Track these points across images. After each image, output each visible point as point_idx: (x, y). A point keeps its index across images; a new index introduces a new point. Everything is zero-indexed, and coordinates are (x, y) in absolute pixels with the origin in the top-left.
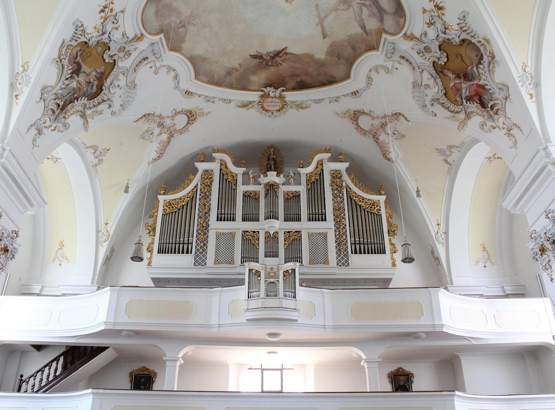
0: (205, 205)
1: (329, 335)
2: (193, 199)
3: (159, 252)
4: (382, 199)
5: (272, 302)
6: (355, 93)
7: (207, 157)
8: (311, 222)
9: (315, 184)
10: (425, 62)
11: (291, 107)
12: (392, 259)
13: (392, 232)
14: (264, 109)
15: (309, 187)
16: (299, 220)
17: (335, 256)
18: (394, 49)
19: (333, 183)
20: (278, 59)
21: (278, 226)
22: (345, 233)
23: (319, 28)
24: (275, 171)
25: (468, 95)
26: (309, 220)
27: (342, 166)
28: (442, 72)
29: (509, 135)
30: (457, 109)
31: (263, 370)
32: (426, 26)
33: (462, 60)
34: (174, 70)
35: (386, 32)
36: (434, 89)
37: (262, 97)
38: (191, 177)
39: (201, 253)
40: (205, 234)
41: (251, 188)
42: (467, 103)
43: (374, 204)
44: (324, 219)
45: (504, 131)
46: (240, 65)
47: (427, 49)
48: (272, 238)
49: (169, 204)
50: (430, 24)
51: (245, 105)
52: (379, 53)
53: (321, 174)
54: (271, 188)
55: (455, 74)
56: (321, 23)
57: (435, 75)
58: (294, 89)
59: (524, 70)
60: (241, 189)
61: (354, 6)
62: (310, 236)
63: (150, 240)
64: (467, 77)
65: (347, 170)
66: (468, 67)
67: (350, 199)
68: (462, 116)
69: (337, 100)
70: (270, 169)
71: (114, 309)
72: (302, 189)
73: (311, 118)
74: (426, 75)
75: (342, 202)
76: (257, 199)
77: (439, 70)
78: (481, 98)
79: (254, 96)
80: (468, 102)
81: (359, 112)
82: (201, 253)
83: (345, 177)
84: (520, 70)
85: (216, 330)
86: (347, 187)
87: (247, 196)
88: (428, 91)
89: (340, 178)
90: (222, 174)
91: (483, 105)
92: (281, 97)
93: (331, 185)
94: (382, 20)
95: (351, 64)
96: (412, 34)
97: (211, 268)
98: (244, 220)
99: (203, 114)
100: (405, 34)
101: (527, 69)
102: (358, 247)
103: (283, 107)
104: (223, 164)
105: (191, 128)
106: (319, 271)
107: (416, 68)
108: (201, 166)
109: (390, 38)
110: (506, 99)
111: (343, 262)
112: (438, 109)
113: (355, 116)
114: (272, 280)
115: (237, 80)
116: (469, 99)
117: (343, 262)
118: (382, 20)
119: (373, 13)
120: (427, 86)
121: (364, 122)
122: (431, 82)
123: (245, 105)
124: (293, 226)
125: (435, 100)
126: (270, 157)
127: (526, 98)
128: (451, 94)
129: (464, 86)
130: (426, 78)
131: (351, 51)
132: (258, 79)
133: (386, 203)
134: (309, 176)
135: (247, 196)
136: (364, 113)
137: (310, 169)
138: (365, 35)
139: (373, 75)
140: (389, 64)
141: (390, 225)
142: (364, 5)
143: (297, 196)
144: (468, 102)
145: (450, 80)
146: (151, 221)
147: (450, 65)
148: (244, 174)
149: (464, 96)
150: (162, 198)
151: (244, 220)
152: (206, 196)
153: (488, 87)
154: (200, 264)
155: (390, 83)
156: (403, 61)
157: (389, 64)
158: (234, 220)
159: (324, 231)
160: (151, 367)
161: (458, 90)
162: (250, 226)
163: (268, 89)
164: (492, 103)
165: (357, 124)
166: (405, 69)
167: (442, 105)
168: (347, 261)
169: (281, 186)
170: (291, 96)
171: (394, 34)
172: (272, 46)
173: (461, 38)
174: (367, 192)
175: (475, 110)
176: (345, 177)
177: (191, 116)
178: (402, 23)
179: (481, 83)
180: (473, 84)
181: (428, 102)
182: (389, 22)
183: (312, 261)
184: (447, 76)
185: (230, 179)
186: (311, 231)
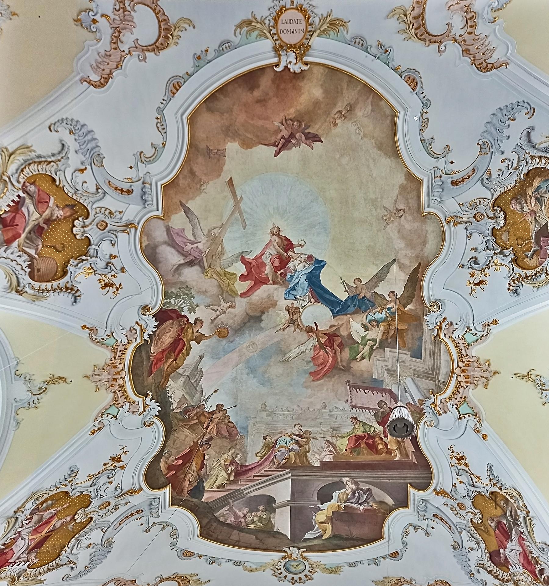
25: (23, 209)
33: (55, 248)
35: (158, 218)
42: (19, 196)
55: (55, 220)
56: (237, 202)
61: (203, 237)
66: (43, 247)
80: (16, 199)
94: (168, 230)
95: (192, 145)
119: (181, 236)
128: (46, 186)
129: (36, 215)
131: (196, 169)
138: (184, 202)
142: (192, 243)
144: (16, 199)
145: (57, 206)
147: (65, 227)
149: (28, 201)
156: (126, 187)
161: (41, 202)
178: (145, 239)
180: (24, 232)
184: (63, 209)
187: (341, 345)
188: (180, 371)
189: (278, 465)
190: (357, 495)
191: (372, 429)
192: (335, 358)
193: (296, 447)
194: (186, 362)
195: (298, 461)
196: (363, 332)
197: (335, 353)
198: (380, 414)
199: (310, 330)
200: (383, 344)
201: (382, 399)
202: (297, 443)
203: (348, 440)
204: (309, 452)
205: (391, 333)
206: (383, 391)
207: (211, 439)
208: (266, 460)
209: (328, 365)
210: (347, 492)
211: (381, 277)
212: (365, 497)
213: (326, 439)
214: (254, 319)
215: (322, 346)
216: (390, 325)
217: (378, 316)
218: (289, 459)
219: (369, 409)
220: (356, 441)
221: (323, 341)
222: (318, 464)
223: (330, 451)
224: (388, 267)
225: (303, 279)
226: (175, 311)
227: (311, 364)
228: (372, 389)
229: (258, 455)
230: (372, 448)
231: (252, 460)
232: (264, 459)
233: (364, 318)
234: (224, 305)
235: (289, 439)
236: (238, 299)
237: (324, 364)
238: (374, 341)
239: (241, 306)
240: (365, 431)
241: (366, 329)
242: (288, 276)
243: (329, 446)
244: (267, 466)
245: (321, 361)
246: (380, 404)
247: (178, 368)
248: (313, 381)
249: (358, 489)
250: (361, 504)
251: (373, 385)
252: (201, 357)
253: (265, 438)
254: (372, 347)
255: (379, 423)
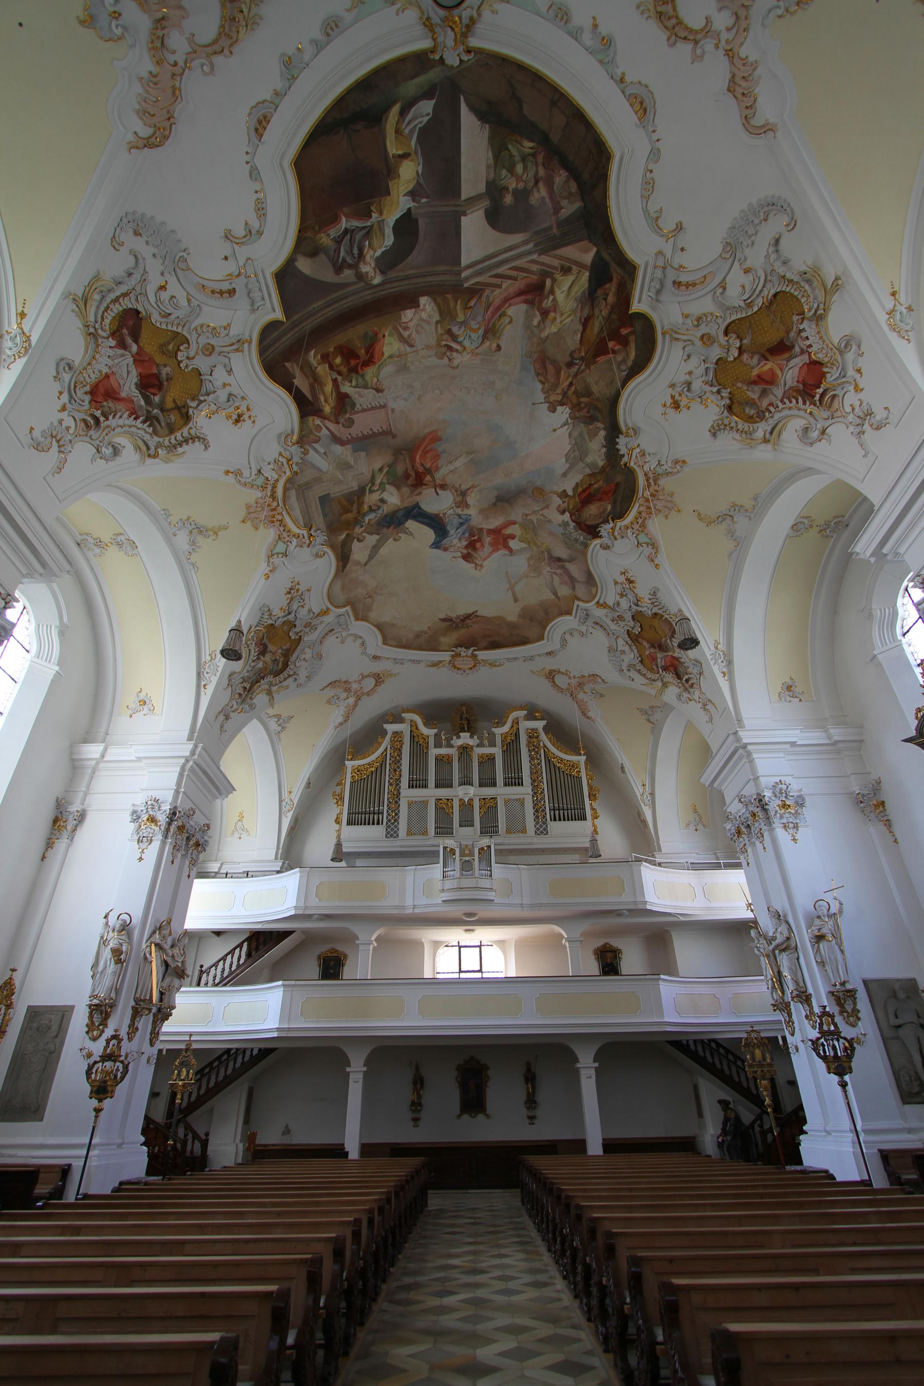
0: (395, 770)
1: (527, 913)
2: (383, 765)
3: (348, 824)
4: (582, 759)
5: (467, 883)
6: (549, 654)
7: (398, 719)
8: (508, 788)
9: (511, 746)
10: (620, 629)
11: (484, 665)
12: (594, 825)
13: (592, 797)
14: (455, 667)
15: (505, 748)
16: (494, 785)
17: (533, 823)
18: (587, 615)
19: (529, 743)
20: (468, 621)
21: (471, 792)
22: (543, 798)
23: (510, 593)
24: (468, 731)
26: (505, 785)
27: (539, 725)
28: (637, 640)
29: (705, 710)
30: (654, 677)
31: (460, 947)
32: (618, 596)
34: (361, 638)
35: (579, 599)
36: (630, 656)
37: (453, 656)
38: (380, 740)
39: (393, 824)
40: (396, 802)
41: (443, 751)
43: (574, 766)
44: (520, 784)
45: (700, 705)
46: (429, 628)
47: (621, 618)
48: (466, 807)
49: (358, 770)
50: (622, 595)
51: (435, 664)
52: (572, 618)
53: (517, 735)
54: (465, 750)
56: (512, 588)
57: (630, 642)
58: (486, 648)
59: (716, 648)
60: (434, 752)
62: (507, 802)
63: (337, 810)
64: (662, 647)
65: (545, 728)
67: (548, 761)
68: (659, 684)
69: (531, 658)
70: (463, 730)
71: (304, 891)
72: (497, 751)
73: (504, 675)
74: (621, 642)
75: (539, 764)
76: (450, 763)
77: (634, 639)
78: (675, 668)
79: (446, 656)
81: (554, 671)
82: (393, 824)
83: (543, 736)
84: (712, 648)
85: (410, 911)
86: (545, 746)
87: (439, 759)
88: (623, 656)
89: (537, 737)
90: (412, 737)
91: (679, 677)
92: (474, 656)
93: (528, 746)
94: (573, 588)
96: (605, 603)
97: (403, 841)
98: (437, 786)
99: (391, 675)
100: (598, 602)
101: (719, 647)
102: (557, 812)
103: (475, 665)
104: (413, 724)
105: (379, 689)
106: (515, 841)
107: (611, 634)
108: (390, 728)
109: (581, 604)
110: (700, 674)
111: (542, 830)
112: (634, 674)
113: (551, 675)
114: (467, 859)
115: (427, 642)
116: (665, 669)
117: (542, 830)
118: (573, 588)
120: (623, 652)
121: (559, 679)
122: (627, 648)
123: (435, 664)
124: (488, 792)
125: (631, 667)
126: (462, 715)
127: (719, 676)
128: (646, 661)
129: (659, 655)
130: (621, 644)
132: (446, 640)
133: (586, 763)
134: (504, 737)
135: (439, 759)
136: (559, 672)
137: (506, 728)
139: (567, 637)
140: (583, 629)
141: (590, 787)
142: (556, 573)
143: (491, 758)
146: (338, 790)
148: (436, 735)
150: (349, 764)
151: (437, 786)
152: (397, 762)
153: (682, 660)
154: (392, 836)
155: (586, 647)
156: (596, 627)
157: (583, 629)
158: (426, 787)
159: (521, 797)
160: (341, 948)
161: (654, 659)
162: (443, 793)
163: (459, 649)
164: (686, 677)
165: (554, 682)
166: (599, 634)
167: (639, 671)
168: (545, 829)
169: (475, 749)
170: (483, 655)
171: (587, 602)
172: (462, 610)
173: (654, 611)
174: (566, 753)
175: (671, 680)
176: (543, 736)
177: (379, 679)
179: (676, 655)
181: (624, 667)
182: (581, 590)
183: (509, 831)
184: (641, 644)
185: (421, 741)
186: (507, 797)
187: (407, 476)
188: (588, 471)
189: (481, 297)
190: (356, 251)
191: (354, 383)
192: (413, 460)
193: (455, 330)
194: (581, 477)
195: (452, 304)
196: (385, 496)
197: (413, 467)
198: (349, 409)
199: (443, 487)
200: (361, 491)
201: (350, 430)
202: (454, 338)
203: (383, 354)
204: (437, 322)
205: (355, 506)
206: (352, 441)
207: (570, 365)
208: (499, 308)
209: (420, 452)
210: (371, 252)
211: (375, 549)
212: (342, 254)
213: (413, 349)
214: (504, 499)
215: (429, 471)
216: (359, 512)
217: (372, 516)
218: (466, 308)
219: (364, 410)
220: (372, 356)
221: (428, 478)
222: (423, 300)
223: (406, 329)
224: (371, 557)
225: (452, 532)
226: (581, 529)
227: (440, 450)
228: (365, 438)
229: (508, 320)
230: (348, 353)
231: (517, 311)
232: (499, 311)
233: (386, 509)
234: (534, 518)
235: (466, 343)
236: (519, 519)
237: (425, 453)
238: (371, 492)
239: (517, 513)
240: (363, 376)
241: (383, 501)
242: (467, 535)
243: (410, 336)
244: (497, 295)
245: (429, 455)
246: (351, 422)
247: (590, 475)
248: (436, 431)
249: (355, 266)
250: (346, 231)
251: (363, 443)
252: (565, 475)
253: (499, 348)
254: (373, 484)
255: (346, 396)
